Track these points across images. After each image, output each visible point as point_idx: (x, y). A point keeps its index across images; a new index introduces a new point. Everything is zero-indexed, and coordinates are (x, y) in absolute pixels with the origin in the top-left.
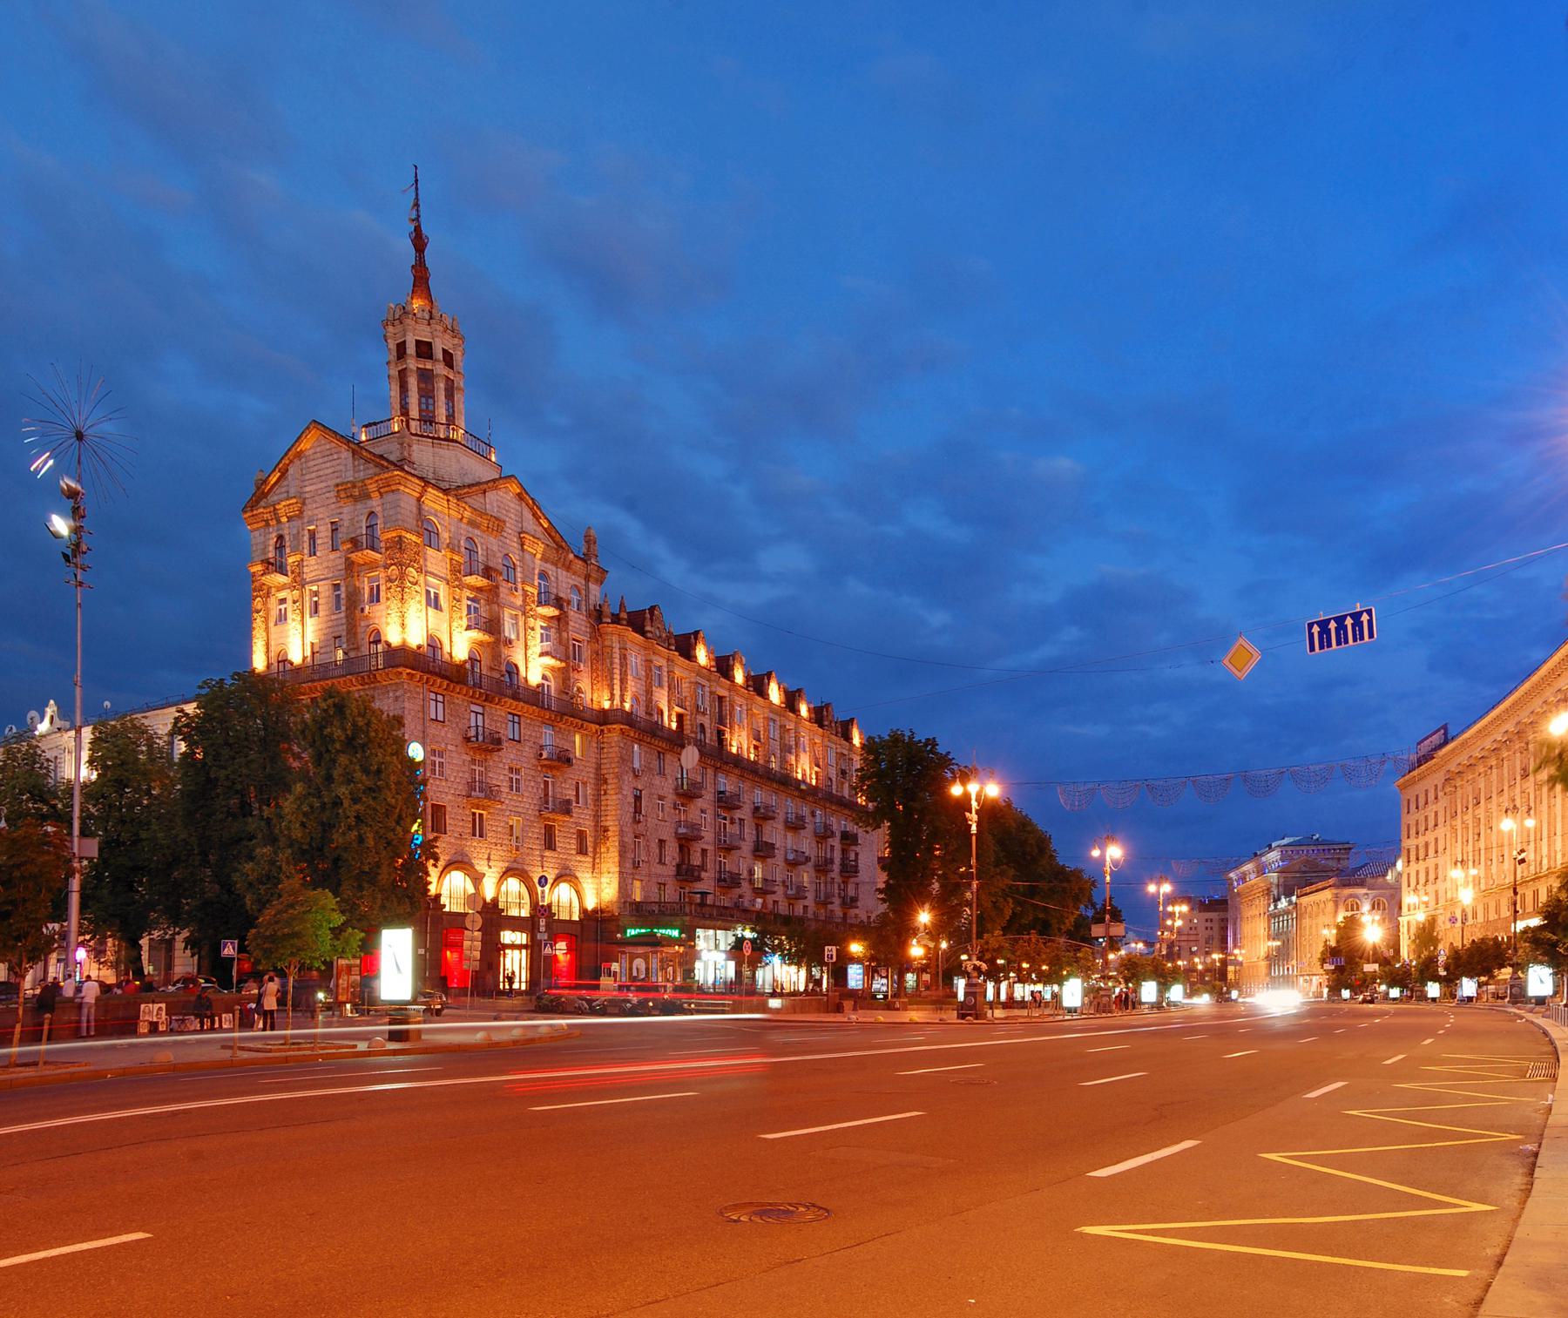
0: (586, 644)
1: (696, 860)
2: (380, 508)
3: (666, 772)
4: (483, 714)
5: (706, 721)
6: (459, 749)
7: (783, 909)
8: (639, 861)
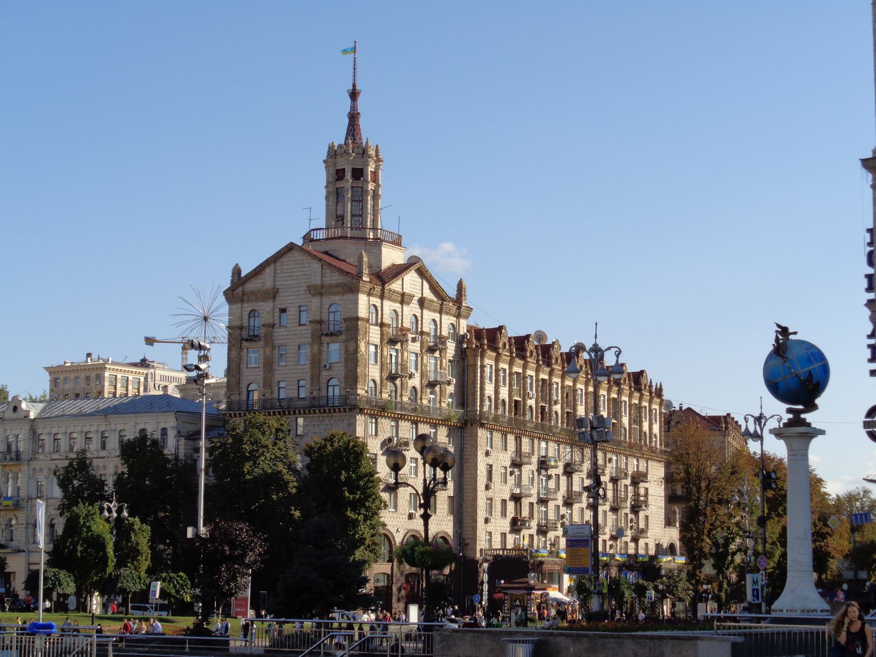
1: (525, 513)
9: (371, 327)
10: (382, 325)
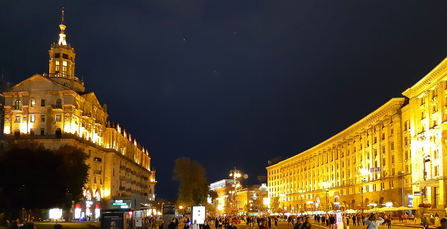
2: (63, 98)
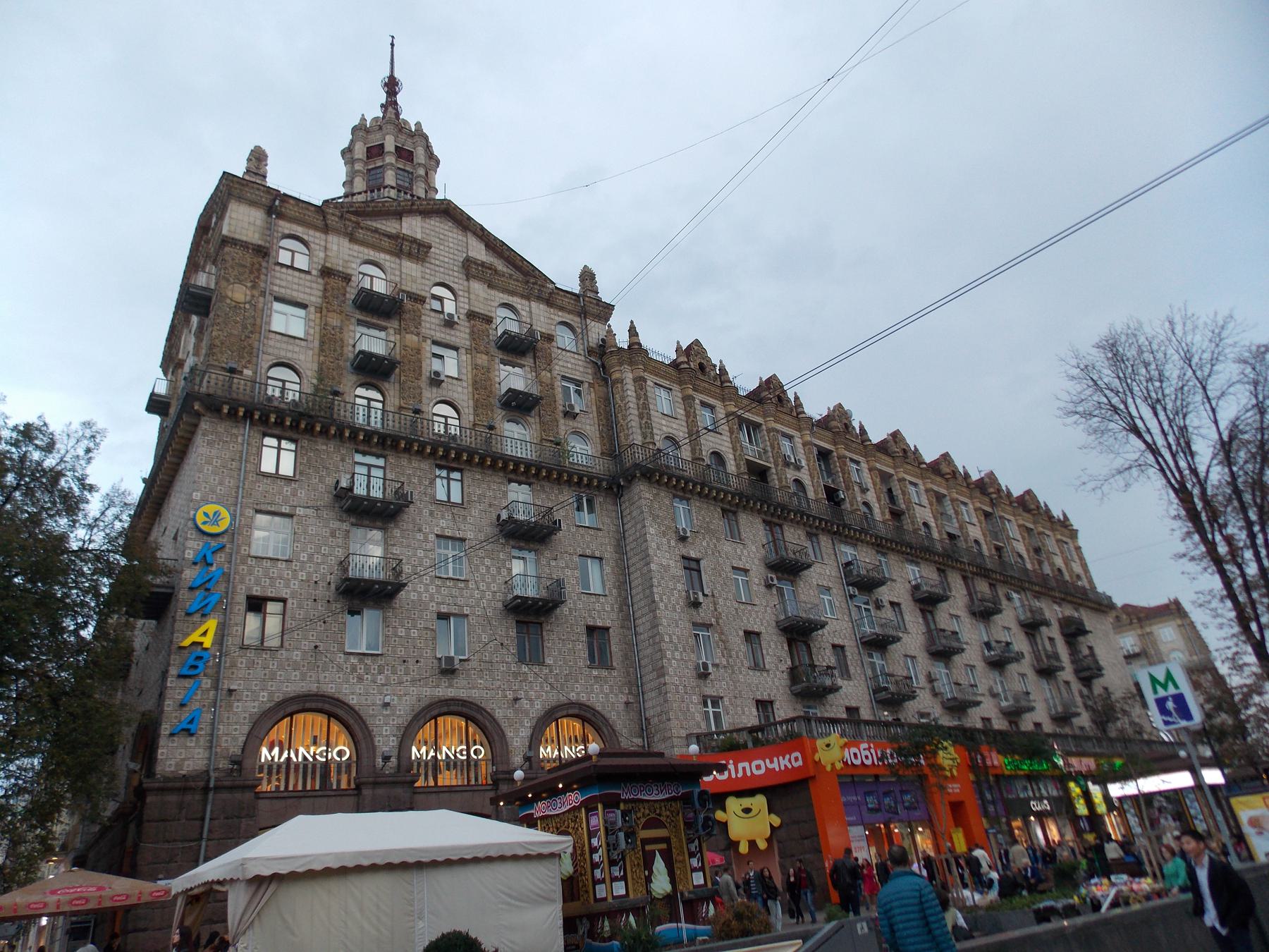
0: (586, 385)
1: (825, 657)
3: (744, 535)
4: (384, 468)
5: (804, 476)
6: (325, 513)
7: (999, 724)
8: (705, 666)
9: (278, 268)
10: (326, 272)
